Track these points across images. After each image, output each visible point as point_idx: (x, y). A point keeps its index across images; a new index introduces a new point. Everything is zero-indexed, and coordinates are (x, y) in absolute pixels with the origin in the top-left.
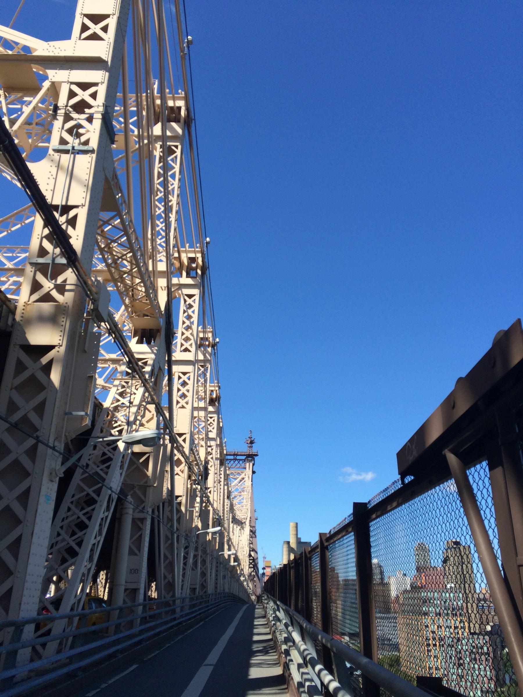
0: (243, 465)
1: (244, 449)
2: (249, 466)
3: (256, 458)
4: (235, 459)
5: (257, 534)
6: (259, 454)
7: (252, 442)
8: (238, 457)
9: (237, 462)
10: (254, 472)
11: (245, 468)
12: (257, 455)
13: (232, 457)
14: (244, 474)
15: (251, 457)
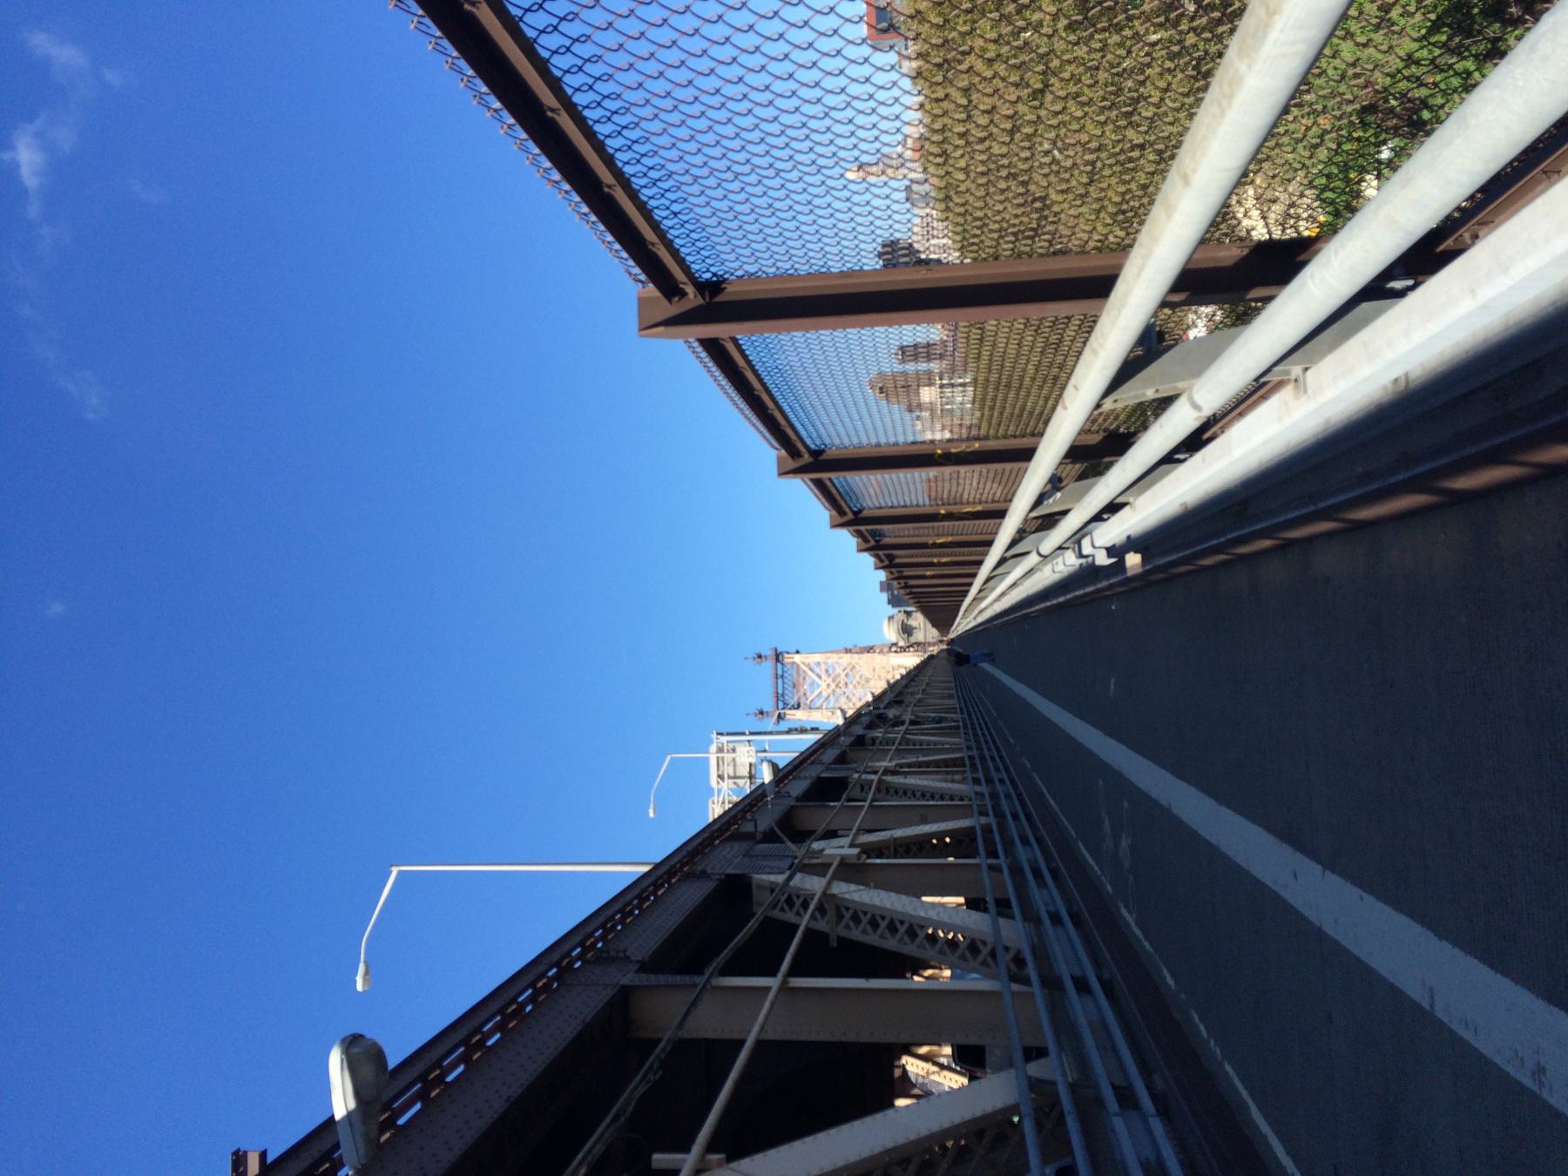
0: (789, 666)
1: (768, 665)
2: (787, 659)
3: (779, 650)
4: (782, 676)
5: (871, 644)
6: (773, 646)
7: (760, 656)
8: (780, 672)
9: (786, 675)
10: (798, 652)
11: (793, 663)
12: (776, 650)
13: (780, 681)
14: (802, 666)
15: (778, 657)
